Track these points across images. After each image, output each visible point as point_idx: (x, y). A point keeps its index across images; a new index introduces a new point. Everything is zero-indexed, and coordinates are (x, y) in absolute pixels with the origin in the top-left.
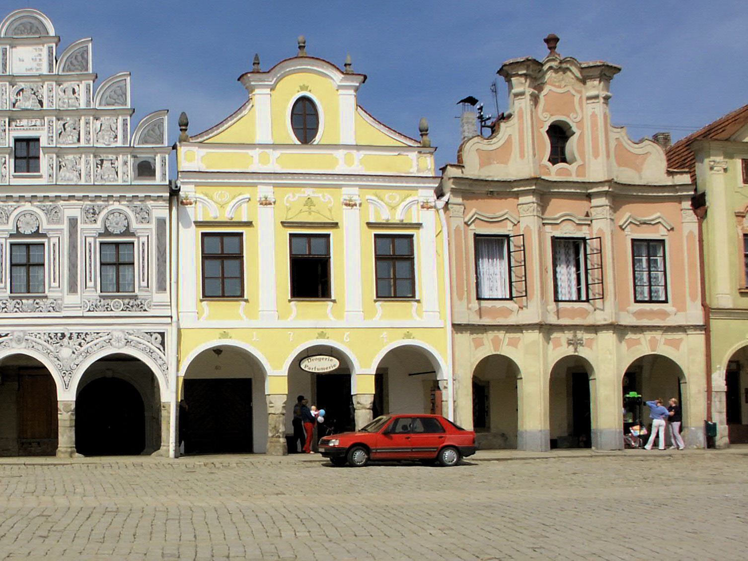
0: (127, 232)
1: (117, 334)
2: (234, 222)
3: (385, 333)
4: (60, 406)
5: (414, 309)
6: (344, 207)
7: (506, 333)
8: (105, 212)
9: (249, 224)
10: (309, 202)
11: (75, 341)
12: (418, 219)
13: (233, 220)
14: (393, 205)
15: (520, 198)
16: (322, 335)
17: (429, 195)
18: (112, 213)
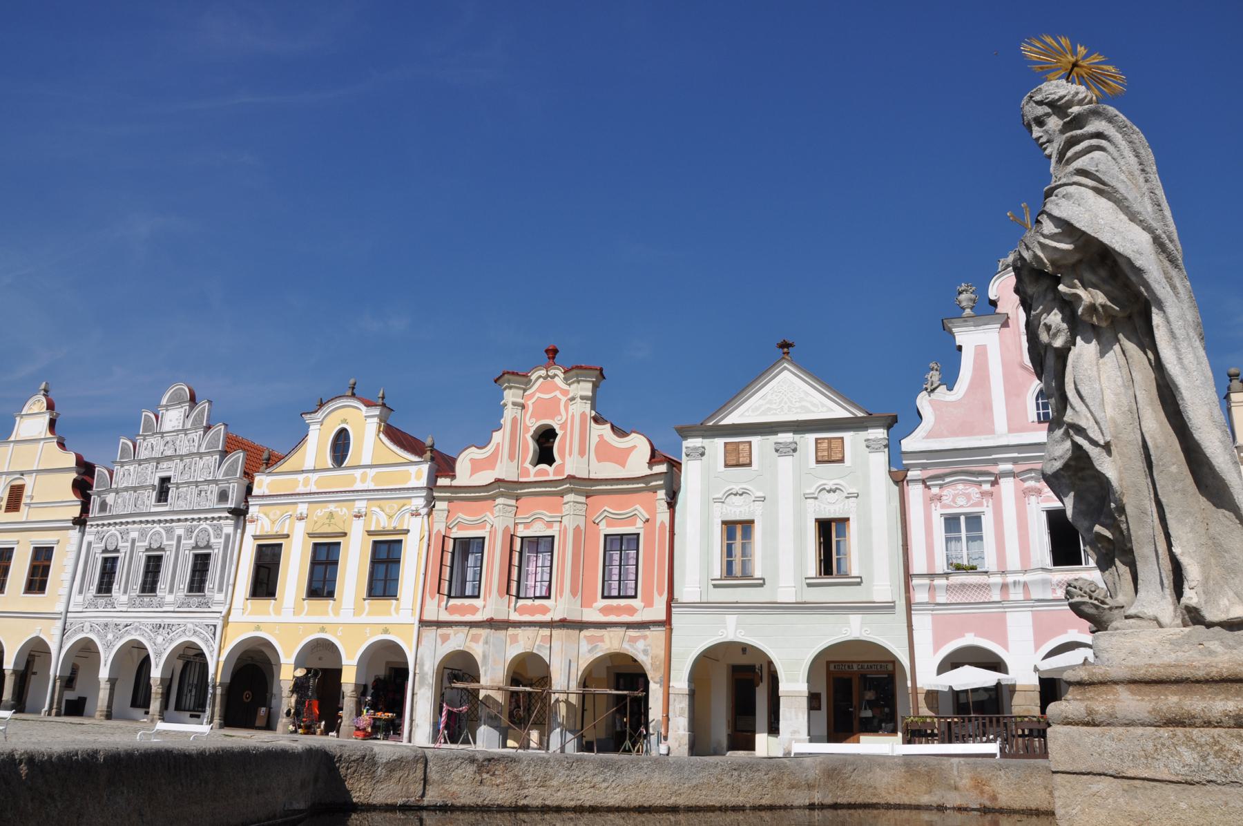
0: (208, 546)
1: (190, 626)
2: (279, 535)
3: (368, 629)
4: (152, 682)
5: (393, 607)
6: (354, 518)
7: (438, 628)
8: (197, 530)
9: (287, 536)
10: (331, 515)
11: (165, 632)
12: (408, 525)
13: (279, 533)
14: (391, 515)
15: (497, 500)
16: (323, 630)
17: (419, 502)
18: (201, 531)
